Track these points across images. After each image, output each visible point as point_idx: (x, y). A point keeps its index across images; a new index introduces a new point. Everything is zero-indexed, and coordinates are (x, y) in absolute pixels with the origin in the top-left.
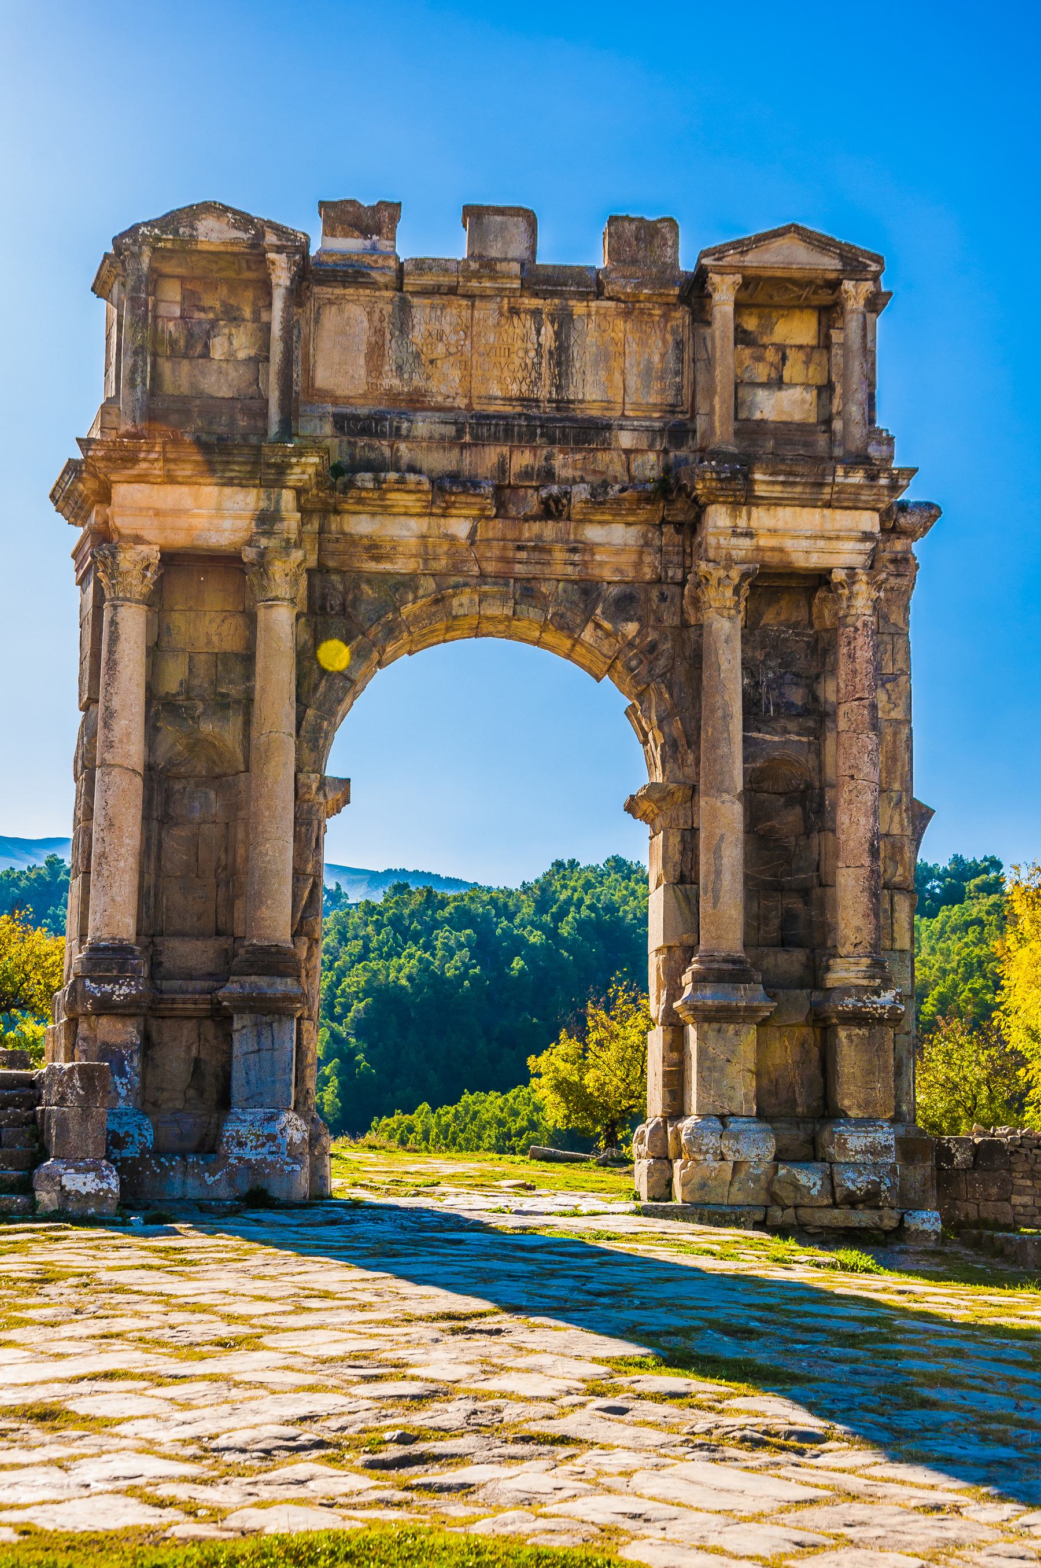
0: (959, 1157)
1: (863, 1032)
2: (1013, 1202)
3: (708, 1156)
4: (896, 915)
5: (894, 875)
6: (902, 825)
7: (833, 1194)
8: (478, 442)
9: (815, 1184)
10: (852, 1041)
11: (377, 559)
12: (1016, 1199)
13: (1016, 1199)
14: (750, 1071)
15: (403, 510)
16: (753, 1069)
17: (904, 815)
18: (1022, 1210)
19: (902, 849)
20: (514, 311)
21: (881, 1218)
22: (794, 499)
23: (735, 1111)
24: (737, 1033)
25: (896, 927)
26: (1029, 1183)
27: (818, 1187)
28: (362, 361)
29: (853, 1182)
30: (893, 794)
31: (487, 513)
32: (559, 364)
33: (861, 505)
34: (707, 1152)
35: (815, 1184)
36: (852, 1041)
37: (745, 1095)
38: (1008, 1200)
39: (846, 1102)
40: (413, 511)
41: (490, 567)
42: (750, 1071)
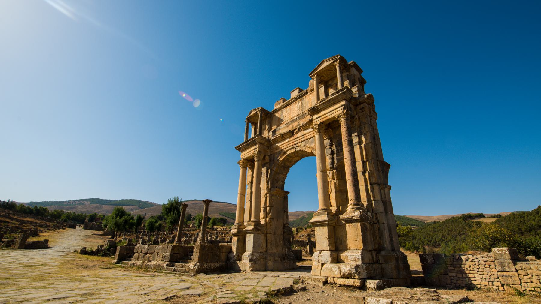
0: (429, 260)
1: (353, 224)
2: (449, 275)
3: (316, 262)
6: (373, 167)
8: (290, 125)
9: (336, 271)
10: (350, 227)
11: (277, 150)
12: (450, 274)
13: (450, 274)
14: (326, 238)
15: (279, 141)
16: (327, 237)
18: (452, 278)
20: (296, 103)
21: (354, 283)
22: (326, 106)
23: (324, 249)
24: (323, 228)
26: (453, 268)
27: (337, 271)
29: (345, 270)
31: (290, 135)
32: (302, 107)
33: (340, 100)
34: (315, 261)
35: (336, 271)
36: (350, 227)
37: (326, 245)
38: (448, 274)
39: (350, 245)
41: (291, 144)
42: (326, 238)
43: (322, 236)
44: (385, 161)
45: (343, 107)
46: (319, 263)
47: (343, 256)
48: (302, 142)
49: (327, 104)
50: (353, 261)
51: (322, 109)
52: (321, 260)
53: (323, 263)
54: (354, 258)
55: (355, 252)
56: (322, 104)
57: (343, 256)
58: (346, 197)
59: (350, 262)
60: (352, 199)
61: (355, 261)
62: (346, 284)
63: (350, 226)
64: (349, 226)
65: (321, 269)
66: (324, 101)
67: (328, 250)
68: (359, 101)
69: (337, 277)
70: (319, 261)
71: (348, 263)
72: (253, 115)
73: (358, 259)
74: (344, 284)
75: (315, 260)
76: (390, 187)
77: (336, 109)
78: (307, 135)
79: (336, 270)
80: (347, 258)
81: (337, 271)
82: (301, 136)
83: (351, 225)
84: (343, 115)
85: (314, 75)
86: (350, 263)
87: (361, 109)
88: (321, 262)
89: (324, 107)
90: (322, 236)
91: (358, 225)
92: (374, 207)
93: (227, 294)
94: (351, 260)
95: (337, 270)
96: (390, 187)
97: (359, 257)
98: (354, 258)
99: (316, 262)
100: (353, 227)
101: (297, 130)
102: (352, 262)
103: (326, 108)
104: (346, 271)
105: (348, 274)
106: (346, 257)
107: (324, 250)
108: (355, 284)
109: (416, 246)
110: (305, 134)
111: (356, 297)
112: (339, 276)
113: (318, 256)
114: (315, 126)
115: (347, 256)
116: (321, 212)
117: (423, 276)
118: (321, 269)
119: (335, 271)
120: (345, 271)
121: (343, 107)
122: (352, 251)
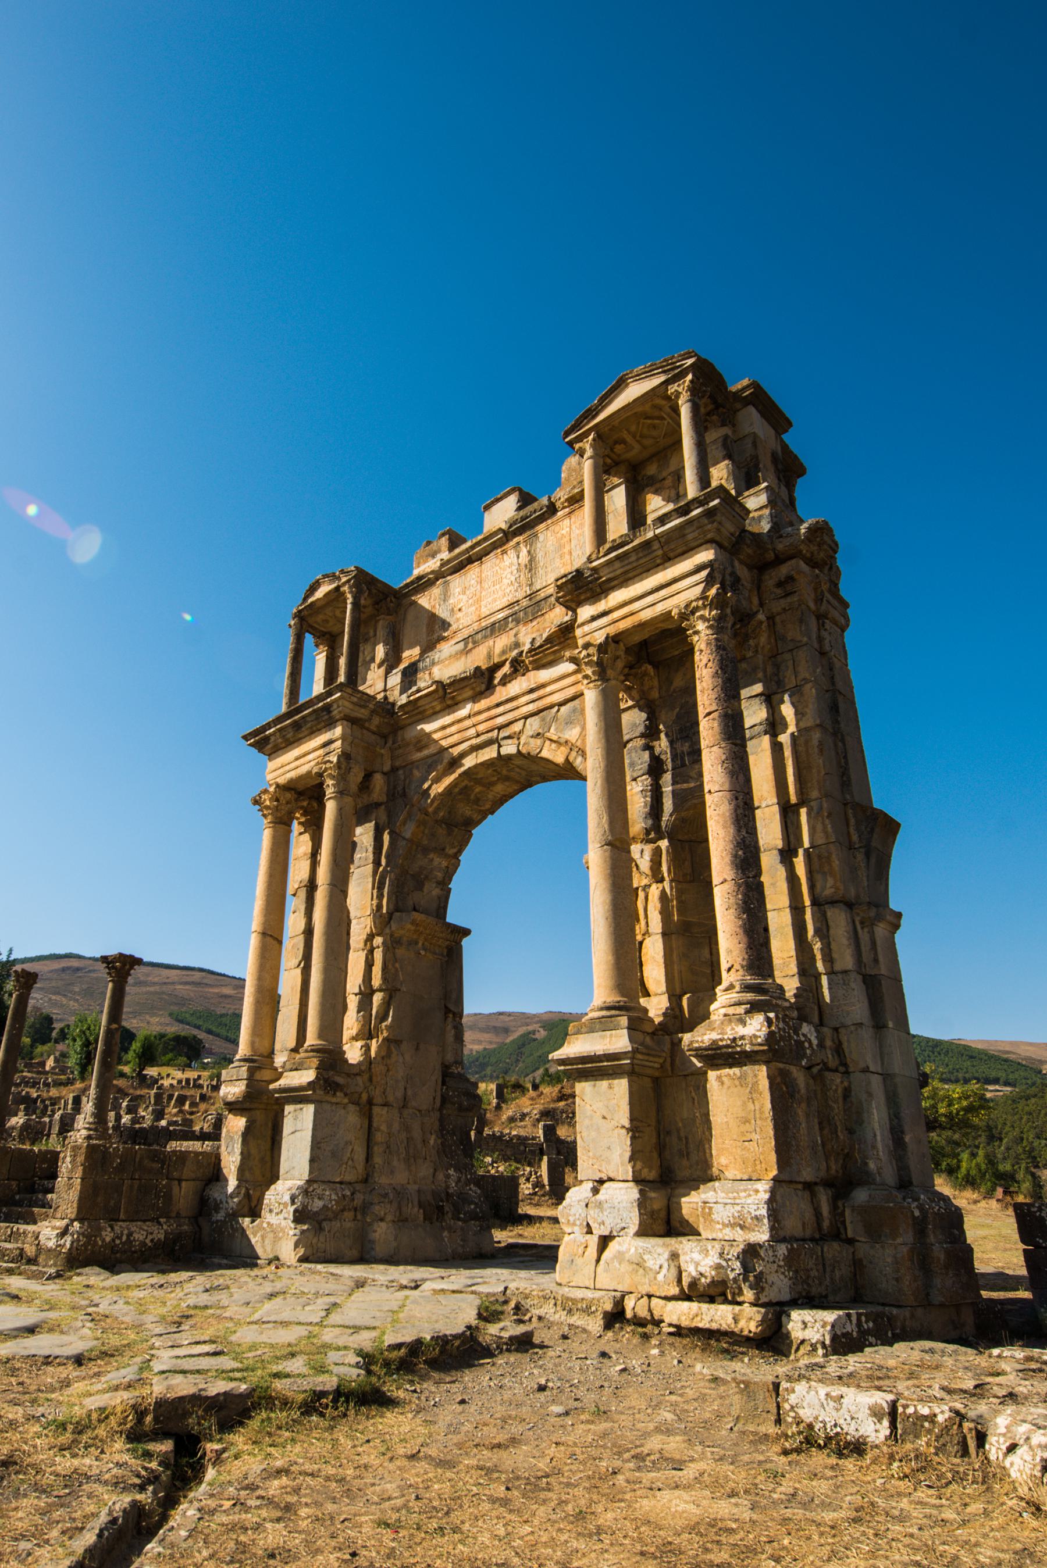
1: (736, 1071)
3: (576, 1229)
4: (832, 932)
5: (824, 888)
7: (679, 1280)
8: (476, 644)
9: (661, 1267)
10: (722, 1083)
14: (623, 1127)
16: (627, 1125)
17: (827, 821)
19: (828, 858)
20: (504, 552)
22: (634, 569)
23: (612, 1175)
24: (610, 1087)
25: (833, 946)
28: (424, 630)
29: (697, 1264)
30: (812, 804)
31: (478, 689)
32: (530, 570)
34: (574, 1224)
35: (661, 1267)
36: (722, 1083)
37: (621, 1156)
39: (723, 1161)
40: (438, 708)
41: (481, 728)
43: (604, 1118)
44: (876, 805)
45: (704, 574)
46: (589, 1231)
47: (690, 1204)
48: (526, 718)
49: (638, 560)
50: (732, 1225)
51: (616, 582)
52: (599, 1221)
53: (607, 1233)
54: (736, 1214)
55: (745, 1191)
56: (617, 558)
57: (690, 1204)
58: (708, 956)
59: (721, 1230)
60: (737, 966)
61: (742, 1227)
62: (701, 1325)
63: (725, 1079)
64: (719, 1078)
65: (598, 1261)
66: (626, 548)
67: (630, 1178)
68: (774, 549)
69: (663, 1295)
70: (588, 1224)
71: (714, 1236)
72: (323, 603)
73: (757, 1218)
74: (693, 1325)
75: (571, 1219)
76: (899, 915)
77: (675, 581)
78: (548, 689)
79: (658, 1263)
80: (710, 1214)
81: (664, 1271)
82: (523, 694)
83: (729, 1075)
84: (704, 606)
85: (586, 435)
86: (720, 1236)
87: (780, 584)
88: (599, 1231)
89: (622, 570)
90: (604, 1118)
91: (760, 1074)
92: (828, 999)
93: (199, 1355)
94: (725, 1225)
95: (666, 1266)
96: (899, 915)
97: (758, 1213)
98: (736, 1214)
99: (576, 1229)
100: (737, 1082)
101: (506, 669)
102: (727, 1230)
103: (631, 575)
104: (701, 1269)
105: (713, 1283)
106: (703, 1208)
107: (610, 1179)
108: (742, 1323)
109: (1001, 1167)
110: (543, 686)
111: (743, 1382)
112: (675, 1291)
113: (587, 1206)
114: (584, 653)
115: (710, 1208)
116: (603, 1017)
117: (1031, 1297)
118: (598, 1261)
119: (657, 1267)
120: (700, 1269)
121: (704, 574)
122: (730, 1184)
